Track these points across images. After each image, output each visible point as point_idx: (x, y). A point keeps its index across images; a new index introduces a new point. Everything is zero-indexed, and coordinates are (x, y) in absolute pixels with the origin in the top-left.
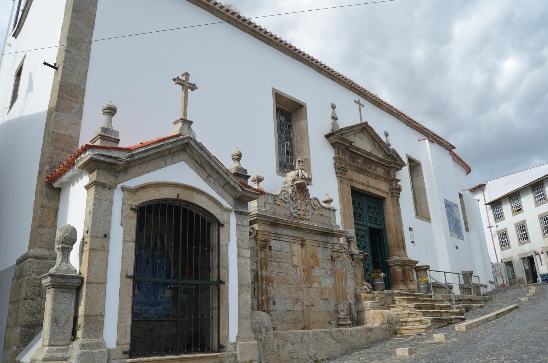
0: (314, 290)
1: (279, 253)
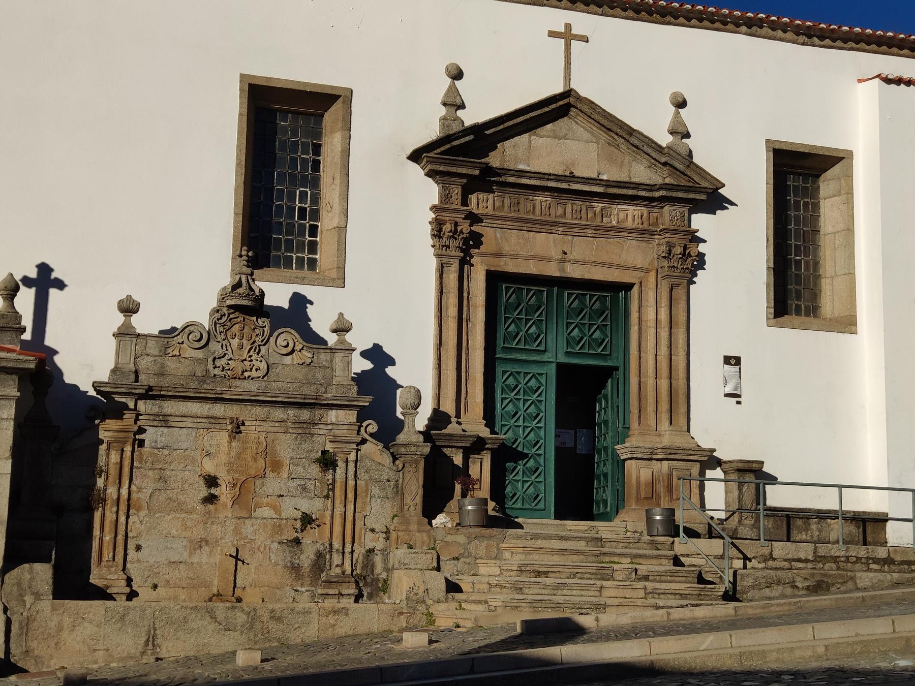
0: (258, 522)
1: (166, 452)
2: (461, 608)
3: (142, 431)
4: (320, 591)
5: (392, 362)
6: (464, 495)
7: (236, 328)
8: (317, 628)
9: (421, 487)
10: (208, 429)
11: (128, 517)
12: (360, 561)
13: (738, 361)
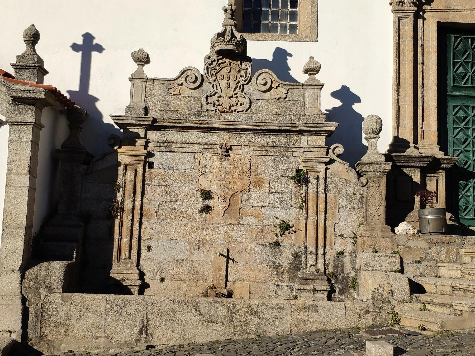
0: (245, 227)
1: (170, 172)
2: (425, 309)
3: (150, 155)
4: (297, 287)
5: (357, 100)
6: (423, 206)
7: (224, 71)
8: (289, 323)
9: (384, 199)
10: (203, 153)
11: (141, 223)
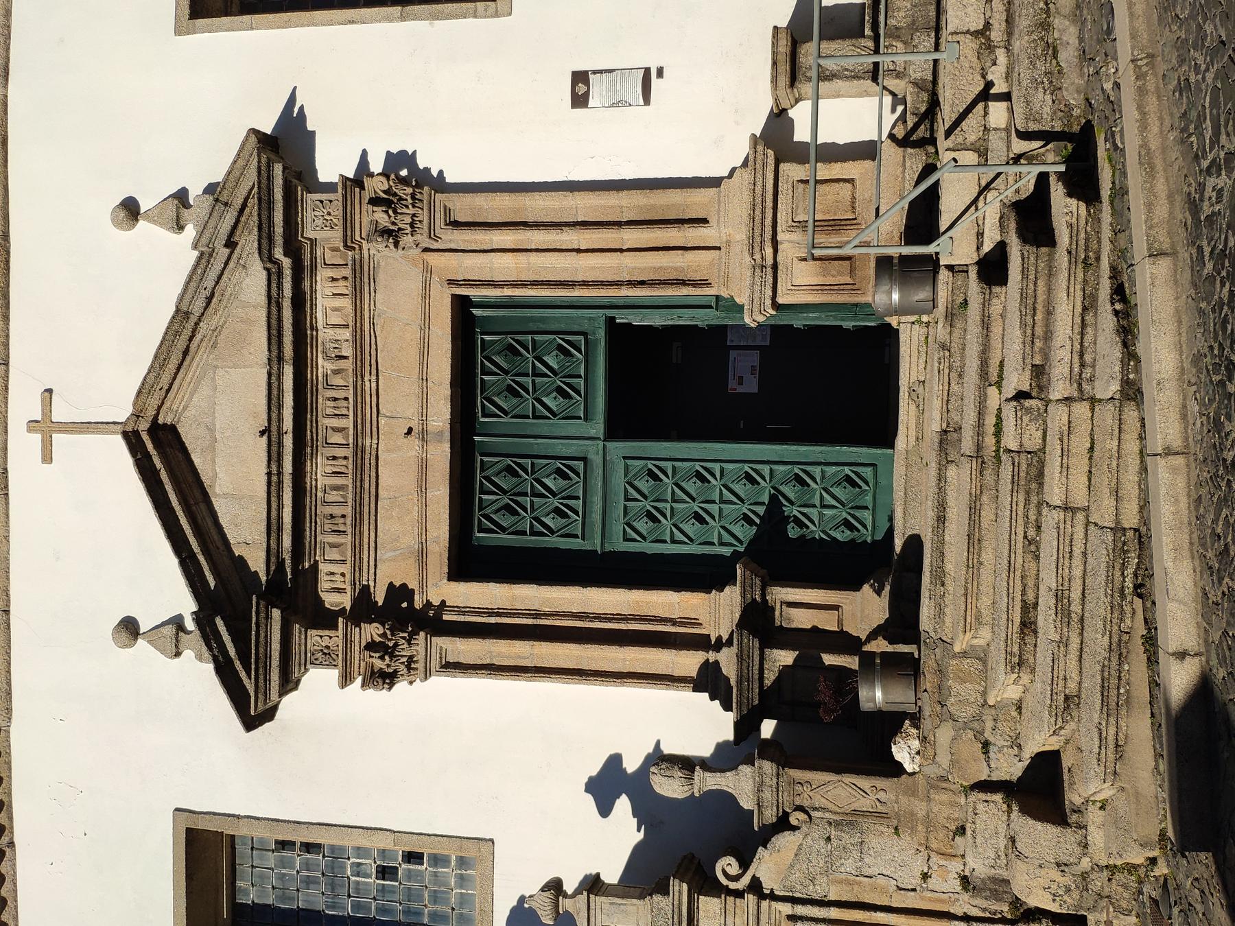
5: (615, 761)
9: (839, 777)
12: (984, 904)
13: (580, 77)
